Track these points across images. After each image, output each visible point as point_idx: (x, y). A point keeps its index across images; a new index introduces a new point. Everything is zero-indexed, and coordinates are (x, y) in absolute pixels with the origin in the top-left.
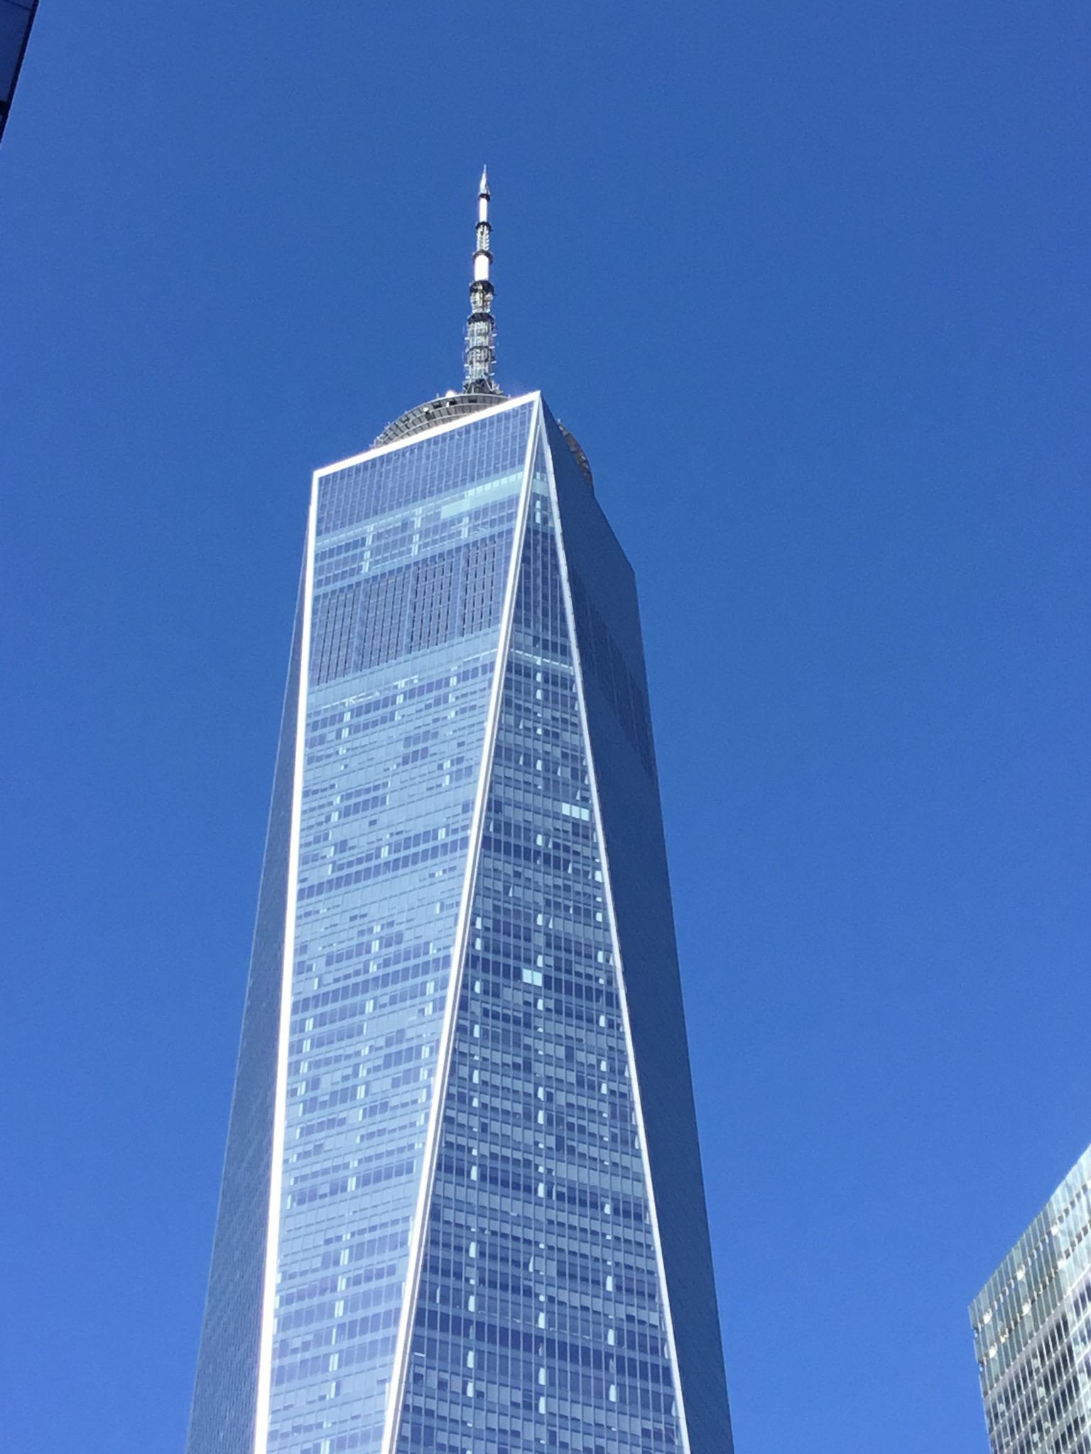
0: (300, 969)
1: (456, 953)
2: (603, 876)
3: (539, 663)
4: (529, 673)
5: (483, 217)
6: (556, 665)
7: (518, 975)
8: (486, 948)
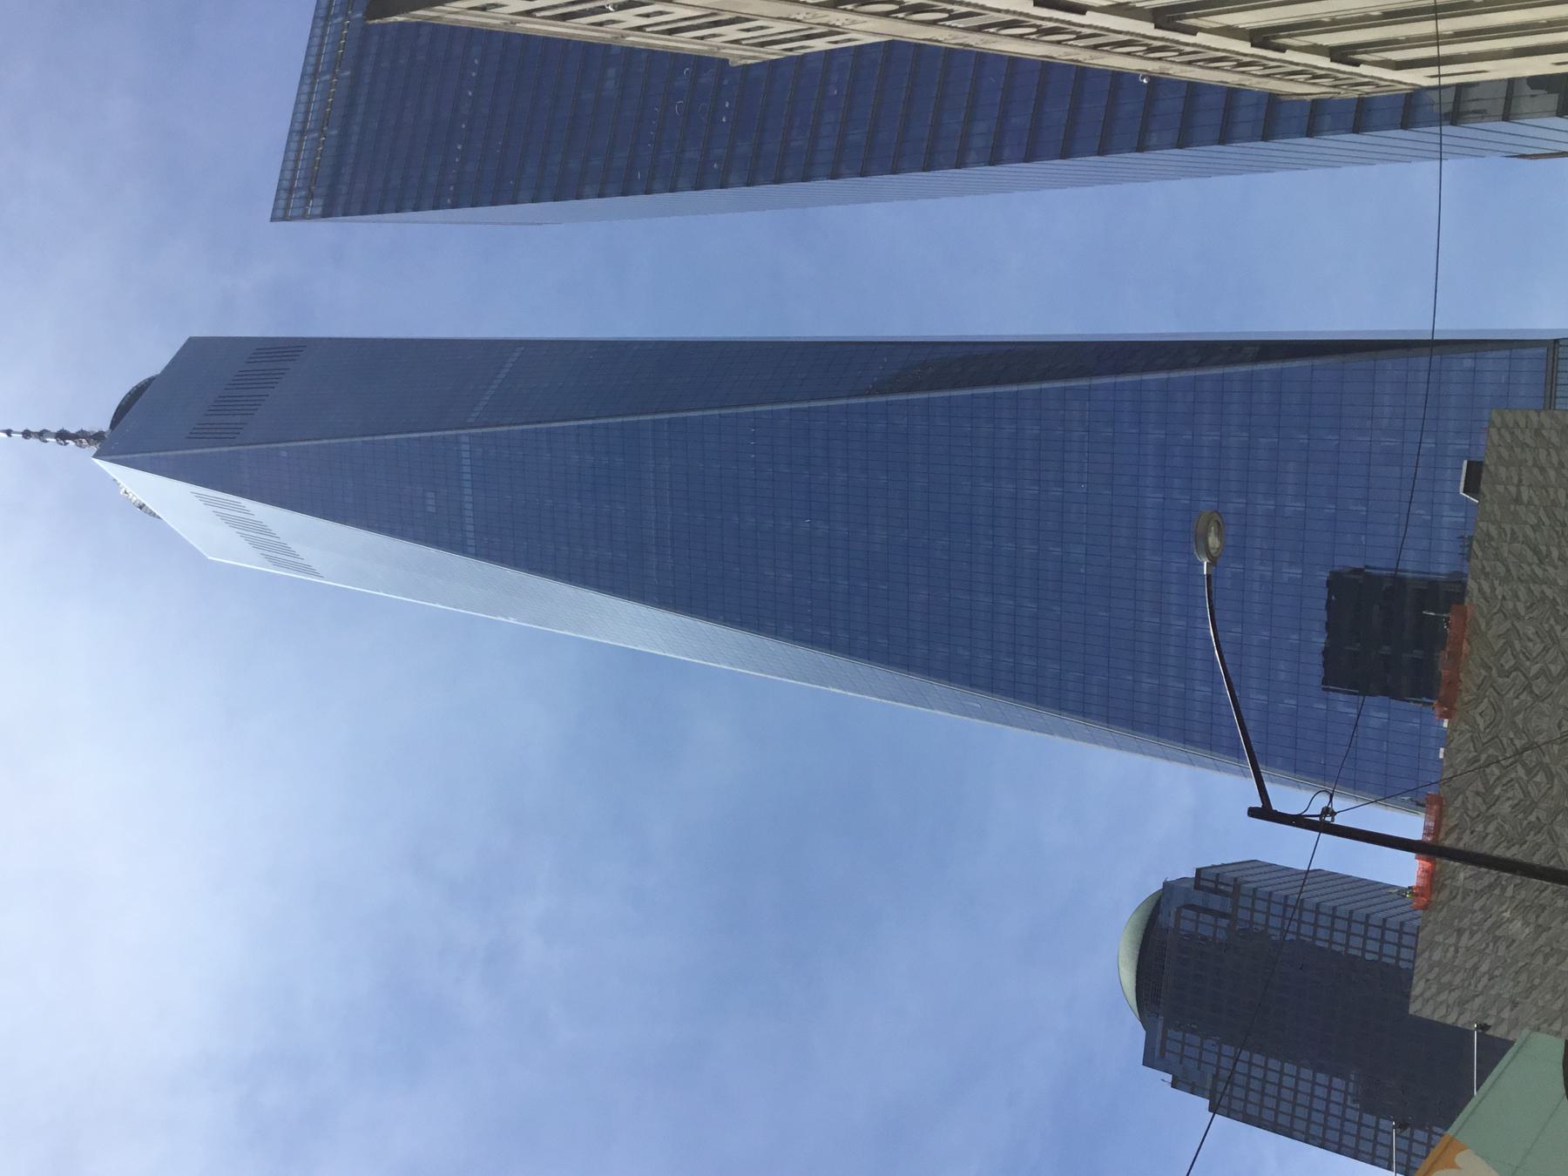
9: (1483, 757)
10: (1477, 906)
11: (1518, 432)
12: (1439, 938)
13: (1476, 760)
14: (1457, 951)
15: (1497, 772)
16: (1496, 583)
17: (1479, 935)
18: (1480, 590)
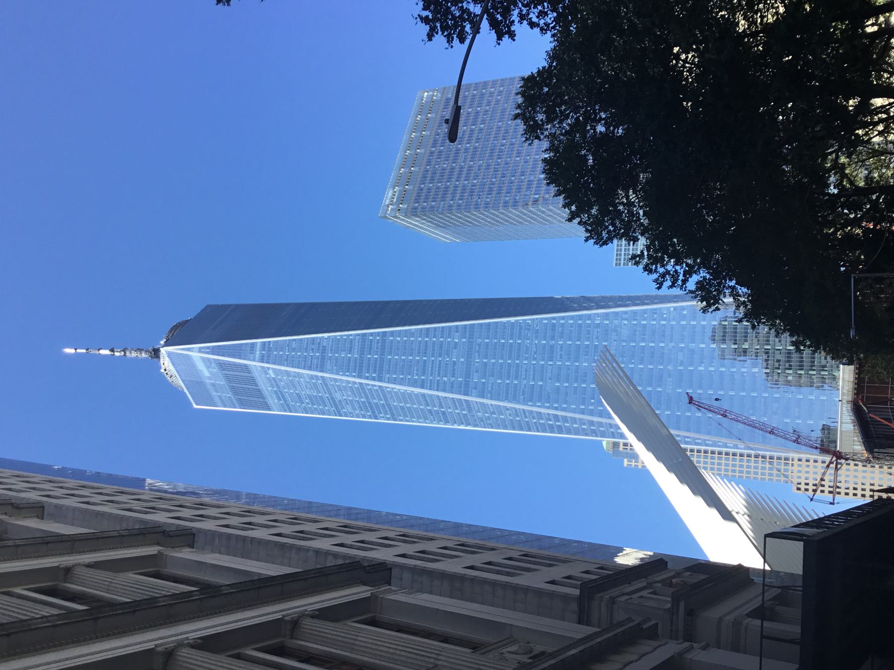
0: (364, 417)
1: (358, 380)
2: (326, 335)
3: (258, 352)
5: (84, 351)
6: (258, 347)
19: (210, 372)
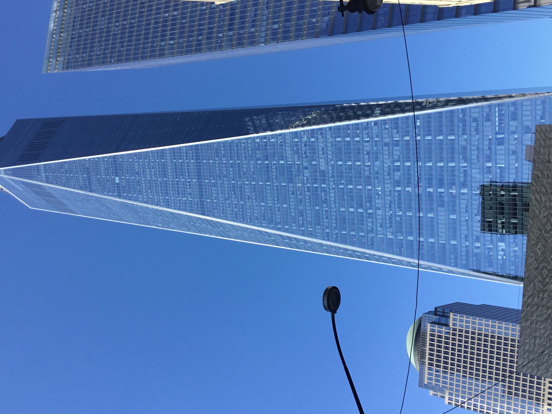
4: (47, 177)
6: (42, 168)
7: (117, 184)
8: (115, 192)
9: (541, 266)
10: (542, 327)
11: (547, 134)
12: (527, 341)
13: (538, 268)
14: (535, 346)
15: (547, 272)
16: (542, 196)
17: (542, 339)
18: (536, 199)
19: (22, 188)
